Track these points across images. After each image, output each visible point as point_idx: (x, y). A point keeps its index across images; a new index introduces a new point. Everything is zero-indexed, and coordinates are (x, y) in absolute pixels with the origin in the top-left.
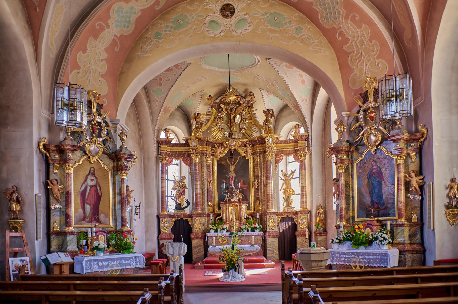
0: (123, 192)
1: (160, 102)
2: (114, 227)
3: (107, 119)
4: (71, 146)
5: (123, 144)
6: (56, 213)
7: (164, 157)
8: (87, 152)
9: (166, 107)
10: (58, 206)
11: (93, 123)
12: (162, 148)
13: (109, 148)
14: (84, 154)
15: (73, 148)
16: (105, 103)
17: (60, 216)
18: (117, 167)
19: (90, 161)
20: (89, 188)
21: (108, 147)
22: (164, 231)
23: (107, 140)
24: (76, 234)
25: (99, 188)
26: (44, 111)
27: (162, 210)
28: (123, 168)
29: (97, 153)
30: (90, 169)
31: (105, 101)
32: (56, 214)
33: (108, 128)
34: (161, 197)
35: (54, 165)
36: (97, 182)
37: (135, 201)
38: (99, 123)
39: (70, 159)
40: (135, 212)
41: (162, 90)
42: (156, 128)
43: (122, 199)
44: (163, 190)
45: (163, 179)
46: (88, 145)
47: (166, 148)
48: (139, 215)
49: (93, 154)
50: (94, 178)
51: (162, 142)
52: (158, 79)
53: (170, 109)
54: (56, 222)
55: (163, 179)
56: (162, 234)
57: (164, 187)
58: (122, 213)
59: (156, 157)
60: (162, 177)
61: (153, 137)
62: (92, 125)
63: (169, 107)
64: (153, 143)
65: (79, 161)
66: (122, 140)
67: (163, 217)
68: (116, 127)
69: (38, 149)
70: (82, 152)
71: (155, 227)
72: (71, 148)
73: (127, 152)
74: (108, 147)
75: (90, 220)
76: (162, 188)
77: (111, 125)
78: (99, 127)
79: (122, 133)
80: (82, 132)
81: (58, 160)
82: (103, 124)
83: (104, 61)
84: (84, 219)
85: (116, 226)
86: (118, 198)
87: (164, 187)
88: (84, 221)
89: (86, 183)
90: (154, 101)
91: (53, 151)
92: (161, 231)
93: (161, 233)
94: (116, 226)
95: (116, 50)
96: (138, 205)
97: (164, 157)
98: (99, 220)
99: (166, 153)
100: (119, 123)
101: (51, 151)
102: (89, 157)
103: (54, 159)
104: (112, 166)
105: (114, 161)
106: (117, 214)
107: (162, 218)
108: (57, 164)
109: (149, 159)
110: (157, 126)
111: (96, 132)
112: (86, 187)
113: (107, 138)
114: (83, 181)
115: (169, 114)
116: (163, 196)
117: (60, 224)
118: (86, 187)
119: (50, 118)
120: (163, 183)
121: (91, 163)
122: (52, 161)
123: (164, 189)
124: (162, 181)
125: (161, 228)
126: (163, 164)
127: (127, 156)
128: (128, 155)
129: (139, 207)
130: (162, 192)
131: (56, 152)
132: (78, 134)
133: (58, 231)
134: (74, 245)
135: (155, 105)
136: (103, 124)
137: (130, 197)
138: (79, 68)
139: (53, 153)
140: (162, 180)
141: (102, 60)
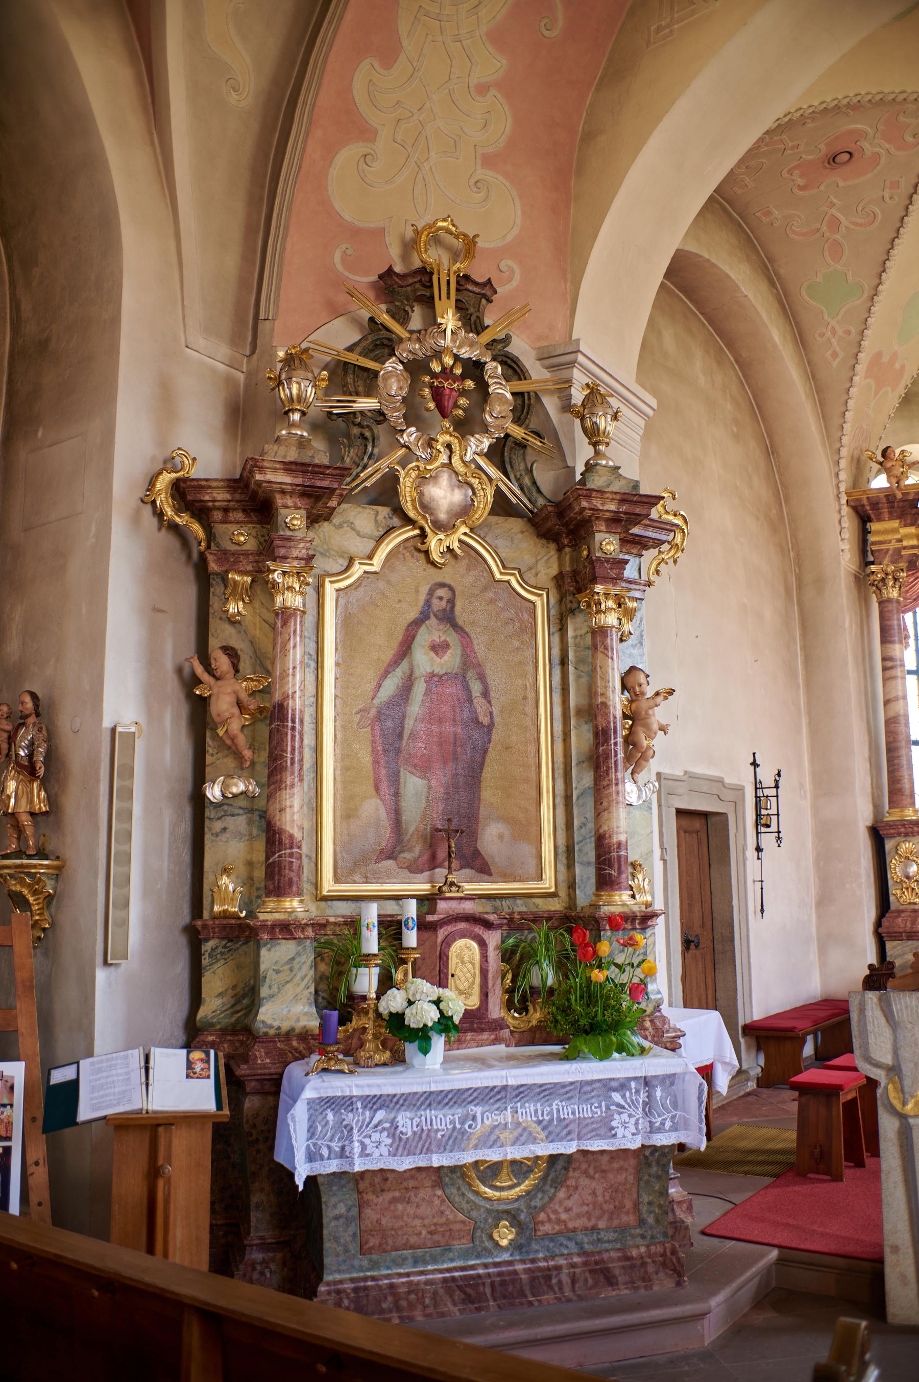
0: (600, 700)
1: (848, 333)
2: (563, 893)
3: (520, 348)
4: (290, 467)
5: (597, 453)
6: (230, 822)
7: (892, 568)
8: (412, 514)
9: (879, 355)
10: (238, 787)
11: (436, 367)
12: (879, 533)
13: (534, 483)
14: (396, 521)
15: (299, 481)
16: (510, 280)
17: (251, 838)
18: (575, 573)
19: (427, 553)
20: (420, 688)
21: (527, 481)
22: (908, 897)
23: (521, 445)
24: (310, 932)
25: (476, 688)
26: (201, 342)
27: (893, 803)
28: (599, 572)
29: (465, 511)
30: (431, 593)
31: (512, 272)
32: (231, 827)
33: (521, 386)
34: (888, 743)
35: (225, 580)
36: (469, 662)
37: (755, 764)
38: (474, 369)
39: (288, 539)
40: (758, 815)
41: (850, 278)
42: (844, 452)
43: (602, 736)
44: (891, 714)
45: (889, 664)
46: (414, 474)
47: (895, 531)
48: (774, 828)
49: (442, 516)
50: (452, 638)
51: (875, 504)
52: (824, 228)
53: (897, 366)
54: (225, 871)
55: (889, 664)
56: (900, 912)
57: (896, 699)
58: (598, 815)
59: (856, 577)
60: (884, 659)
61: (832, 493)
62: (434, 375)
63: (894, 356)
64: (837, 517)
65: (370, 557)
66: (594, 436)
67: (899, 834)
68: (569, 381)
69: (148, 509)
70: (384, 511)
71: (863, 880)
72: (288, 479)
73: (617, 486)
74: (527, 481)
75: (425, 857)
76: (887, 703)
77: (537, 372)
78: (470, 384)
79: (594, 396)
80: (380, 413)
81: (246, 554)
82: (493, 368)
83: (493, 91)
84: (390, 854)
85: (572, 886)
86: (582, 738)
87: (896, 699)
88: (390, 863)
89: (405, 665)
90: (822, 335)
91: (226, 510)
92: (892, 898)
93: (893, 907)
94: (572, 886)
95: (546, 33)
96: (767, 778)
97: (892, 568)
98: (477, 854)
99: (898, 551)
100: (580, 358)
101: (217, 515)
102: (423, 535)
103: (225, 552)
104: (554, 571)
105: (560, 550)
106: (576, 823)
107: (892, 836)
108: (242, 573)
109: (820, 583)
110: (845, 440)
111: (456, 406)
112: (407, 688)
113: (518, 432)
114: (388, 655)
115: (901, 391)
116: (895, 741)
117: (251, 878)
118: (407, 688)
119: (241, 377)
120: (894, 682)
121: (433, 564)
122: (219, 560)
123: (898, 707)
124: (890, 673)
125: (890, 882)
126: (889, 600)
127: (612, 507)
128: (622, 501)
129: (773, 792)
130: (888, 722)
131: (240, 516)
132: (360, 425)
133: (235, 916)
134: (296, 998)
135: (828, 354)
136: (493, 368)
137: (647, 727)
138: (366, 133)
139: (225, 521)
140: (885, 669)
141: (482, 89)
